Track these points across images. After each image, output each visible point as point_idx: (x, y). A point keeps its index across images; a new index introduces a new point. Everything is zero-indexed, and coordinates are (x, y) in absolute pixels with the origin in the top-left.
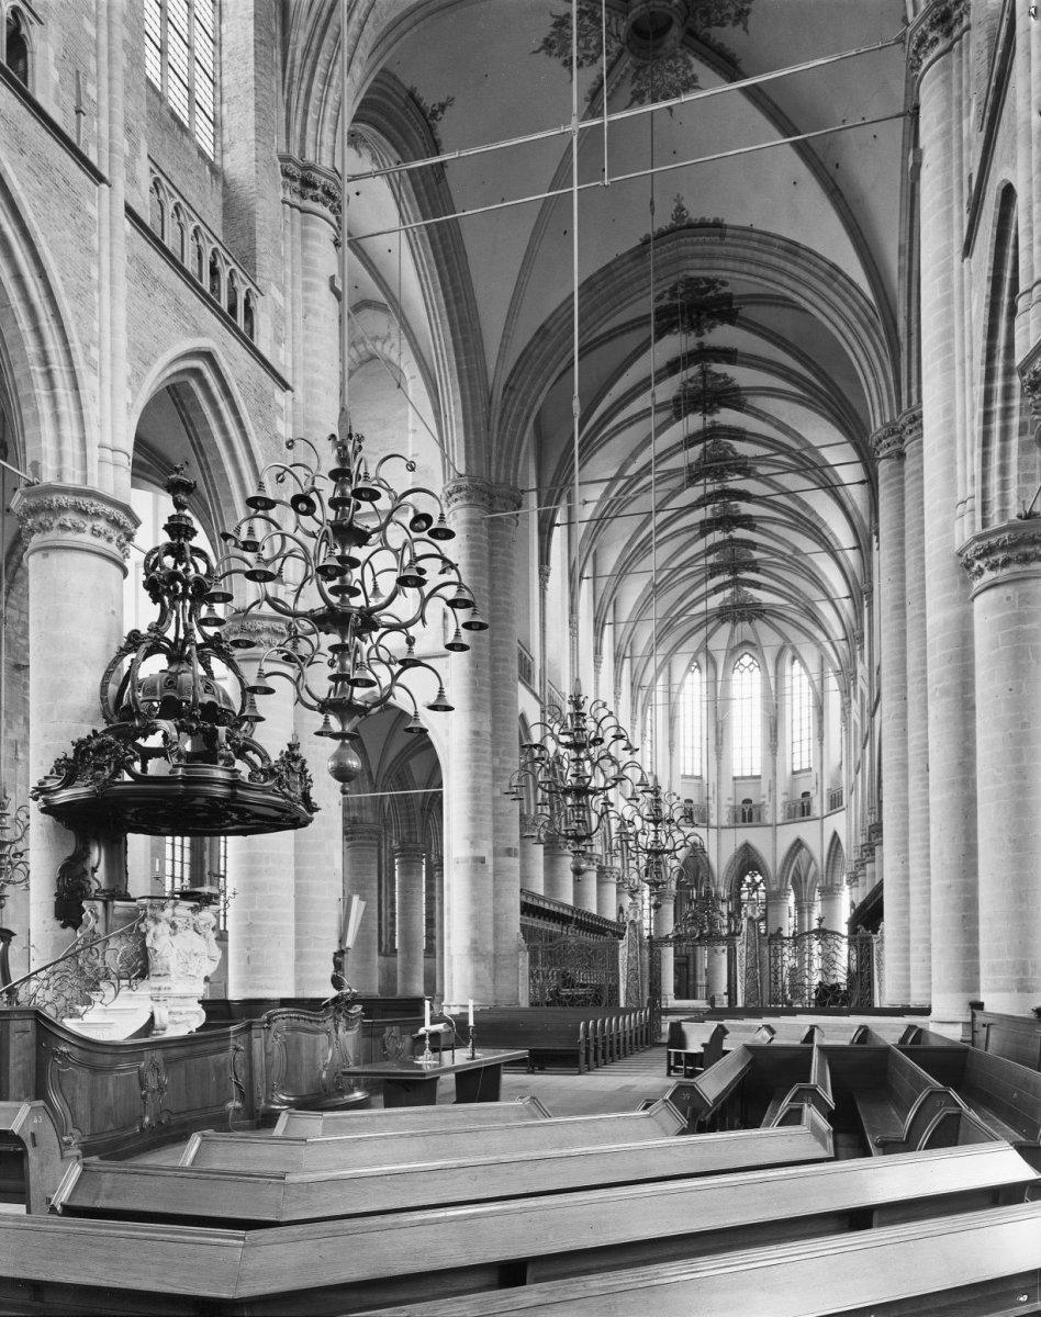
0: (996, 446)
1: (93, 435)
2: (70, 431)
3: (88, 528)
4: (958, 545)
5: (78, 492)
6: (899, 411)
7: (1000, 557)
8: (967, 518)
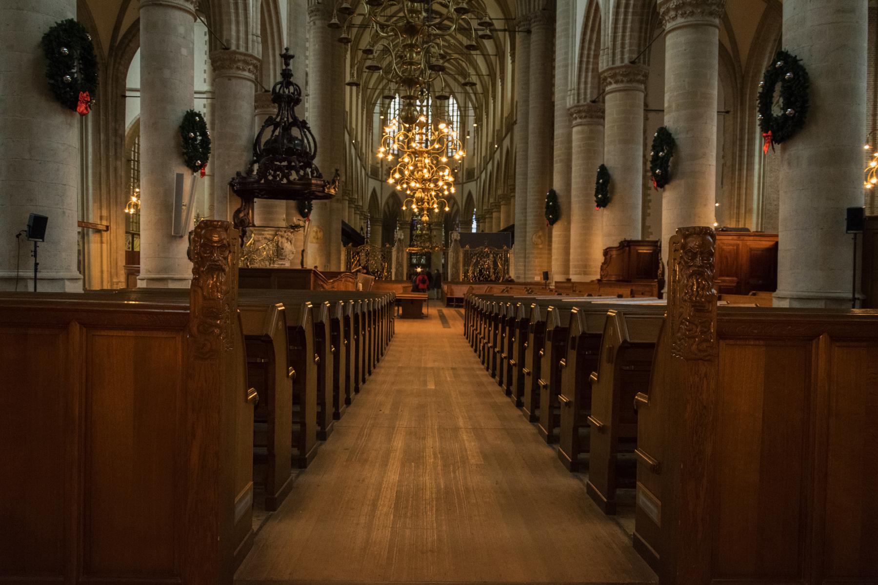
1: (250, 30)
2: (242, 29)
4: (568, 106)
5: (245, 55)
7: (583, 114)
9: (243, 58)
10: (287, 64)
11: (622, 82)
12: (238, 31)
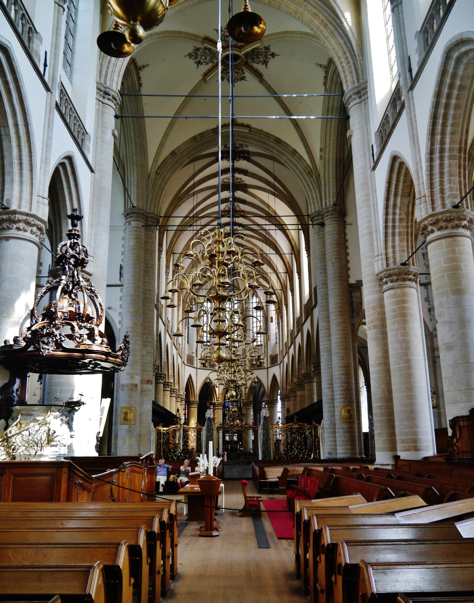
0: (390, 238)
2: (26, 188)
3: (29, 231)
4: (377, 271)
5: (27, 215)
6: (322, 208)
7: (395, 278)
8: (380, 262)
9: (24, 217)
11: (446, 228)
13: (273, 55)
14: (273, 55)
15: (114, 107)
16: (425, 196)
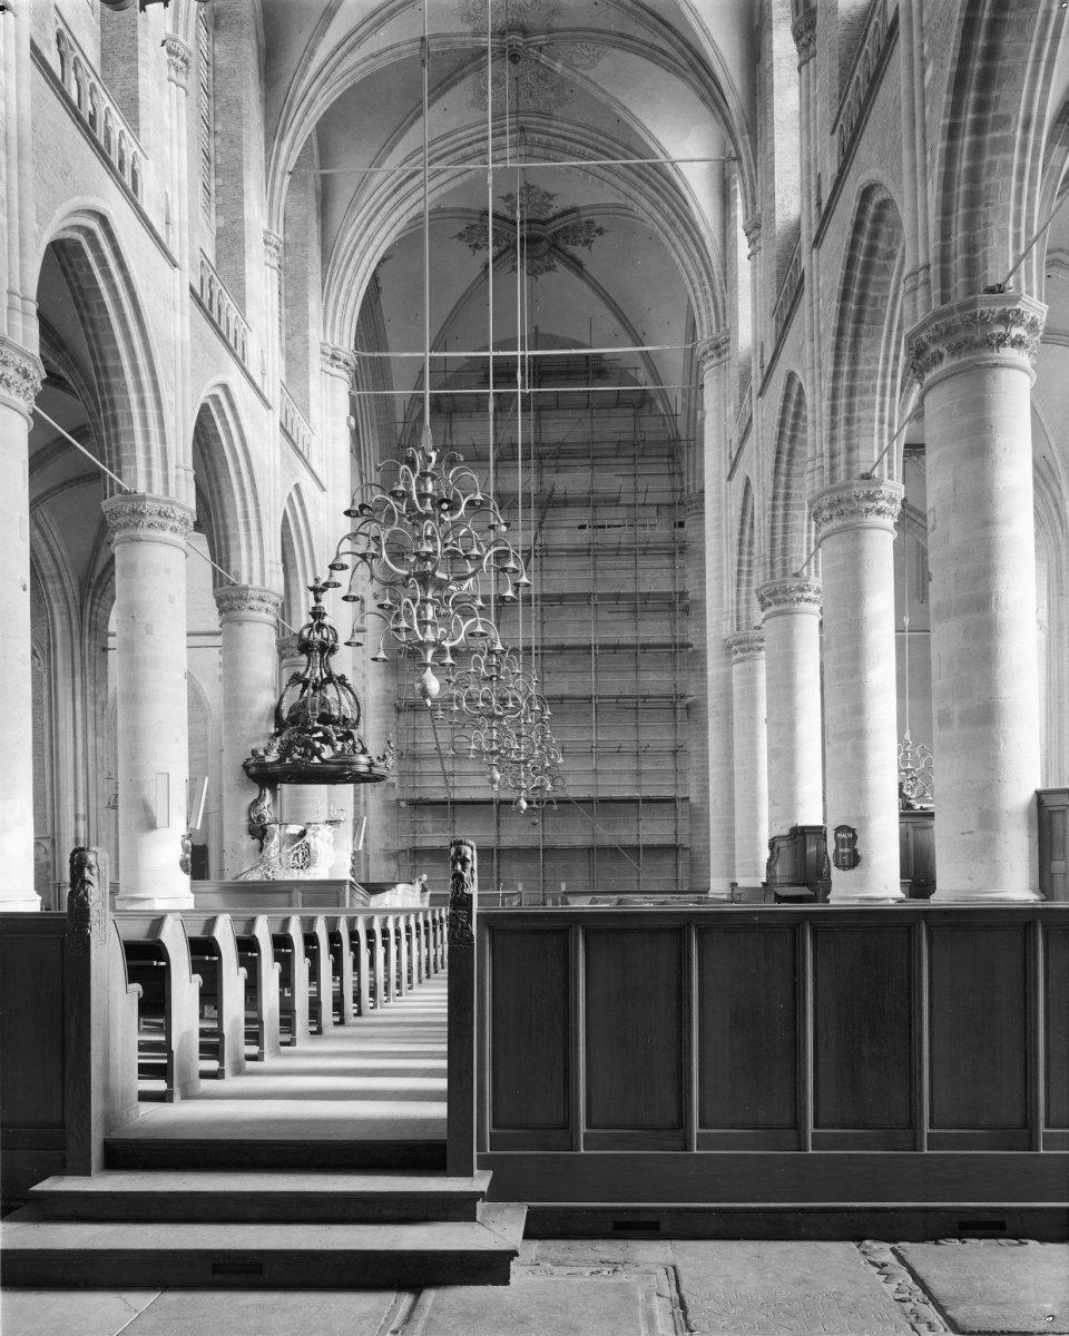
2: (256, 554)
8: (729, 622)
10: (317, 600)
12: (250, 560)
13: (600, 231)
14: (600, 231)
15: (347, 377)
16: (764, 555)
